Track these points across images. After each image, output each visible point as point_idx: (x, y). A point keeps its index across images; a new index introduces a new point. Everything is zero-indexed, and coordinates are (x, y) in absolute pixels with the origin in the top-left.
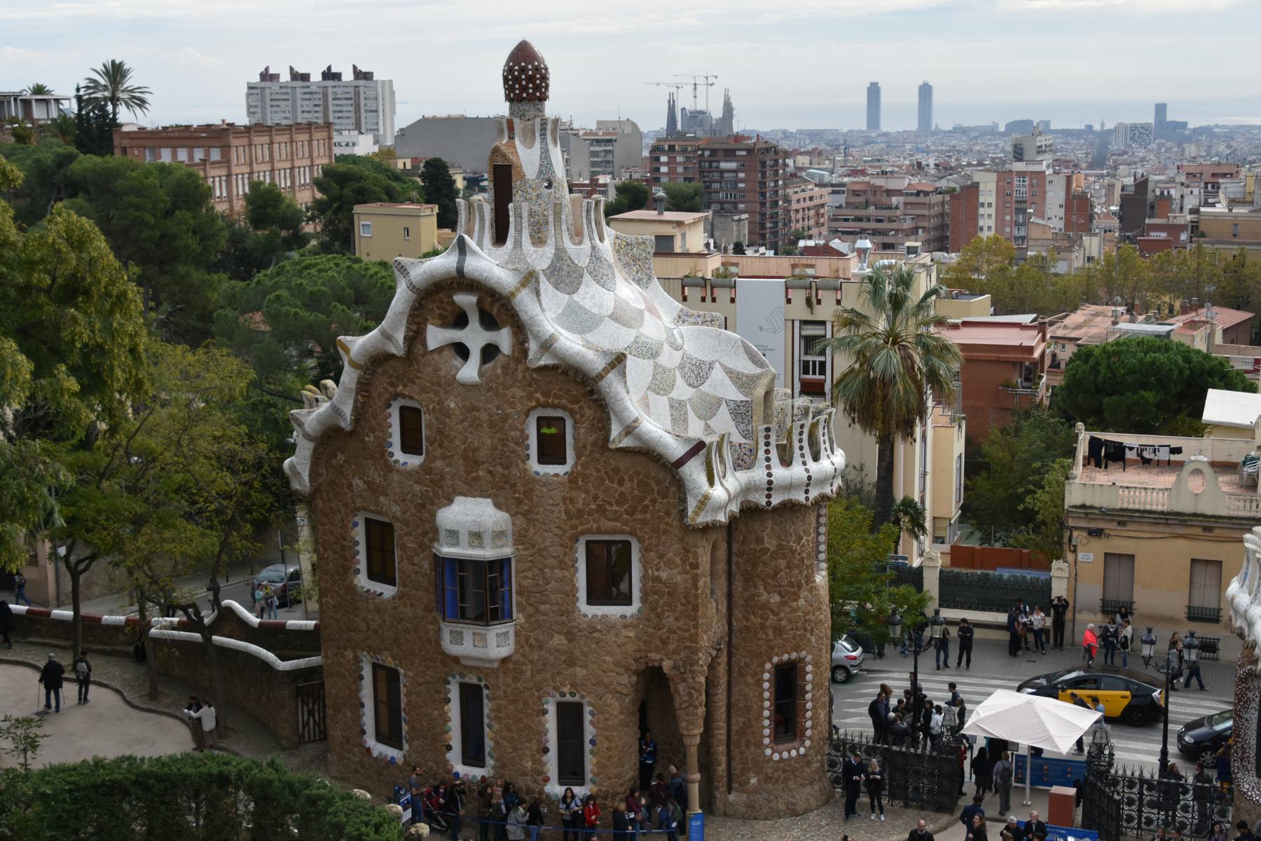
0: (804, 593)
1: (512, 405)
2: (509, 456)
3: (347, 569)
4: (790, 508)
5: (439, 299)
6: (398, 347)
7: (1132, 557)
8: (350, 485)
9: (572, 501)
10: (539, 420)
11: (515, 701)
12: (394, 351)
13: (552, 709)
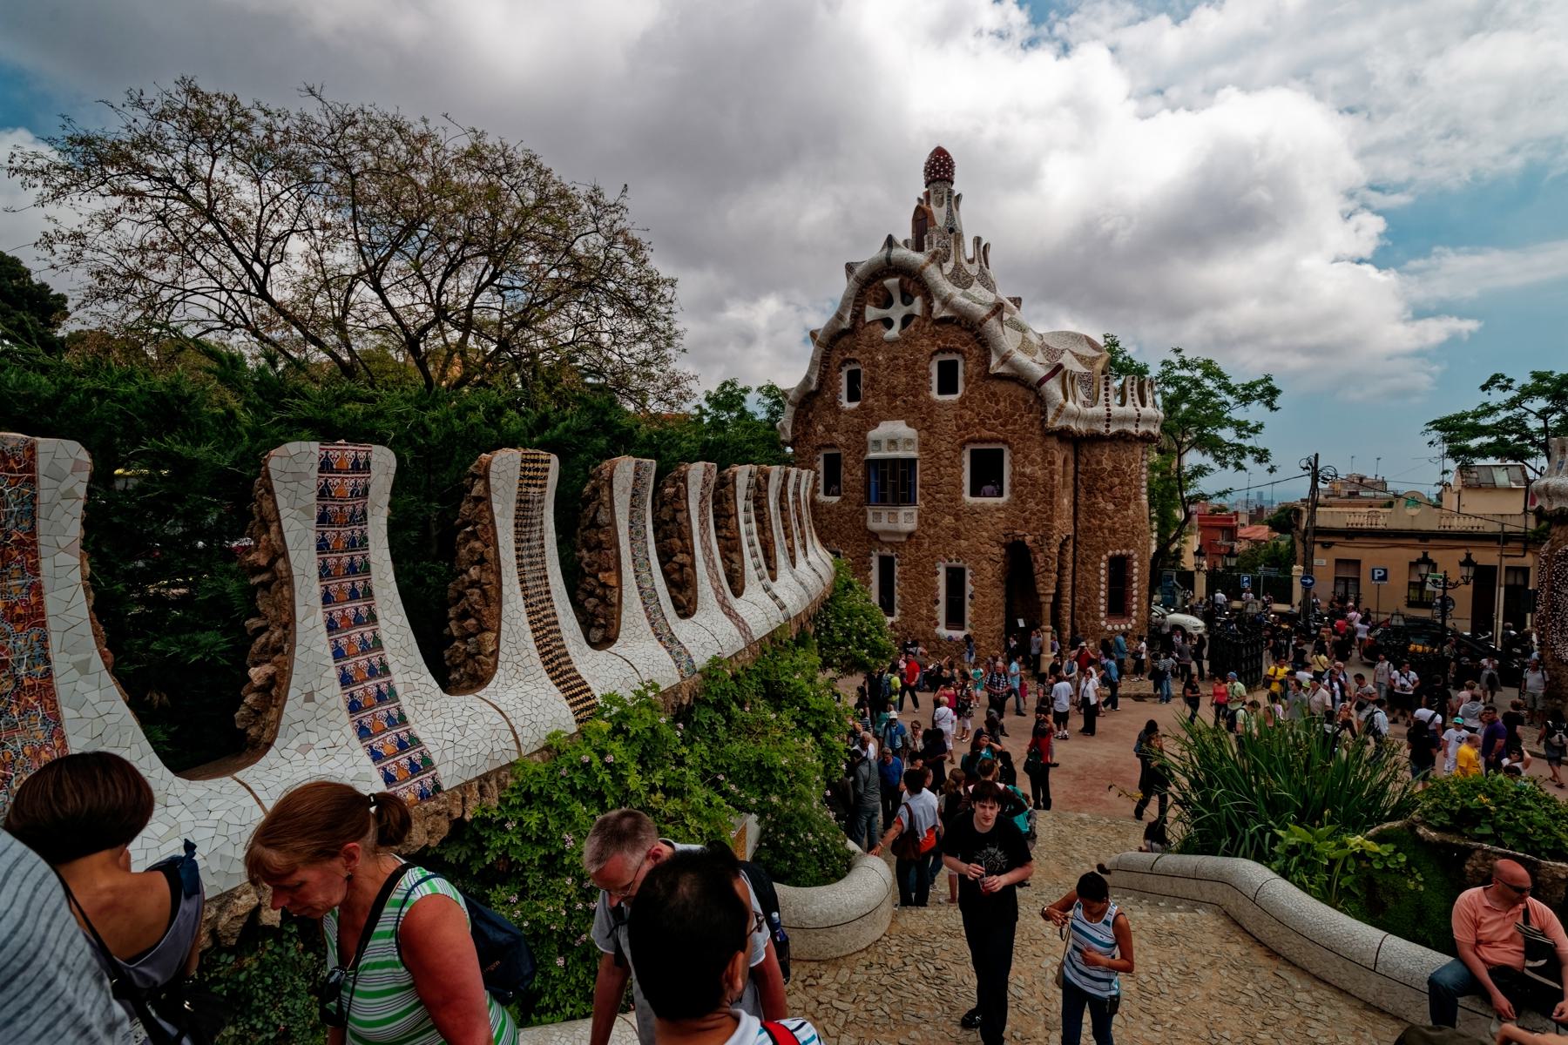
0: (1132, 506)
1: (921, 352)
4: (1123, 438)
6: (847, 323)
9: (961, 417)
10: (941, 364)
13: (942, 571)
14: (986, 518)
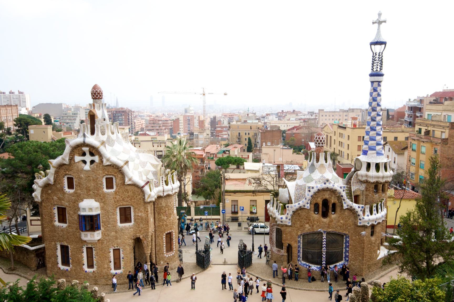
0: (172, 216)
1: (99, 175)
2: (98, 188)
3: (52, 220)
4: (169, 196)
5: (78, 149)
6: (67, 161)
7: (237, 201)
8: (53, 199)
9: (116, 198)
11: (102, 250)
12: (65, 163)
13: (112, 251)
14: (127, 231)
